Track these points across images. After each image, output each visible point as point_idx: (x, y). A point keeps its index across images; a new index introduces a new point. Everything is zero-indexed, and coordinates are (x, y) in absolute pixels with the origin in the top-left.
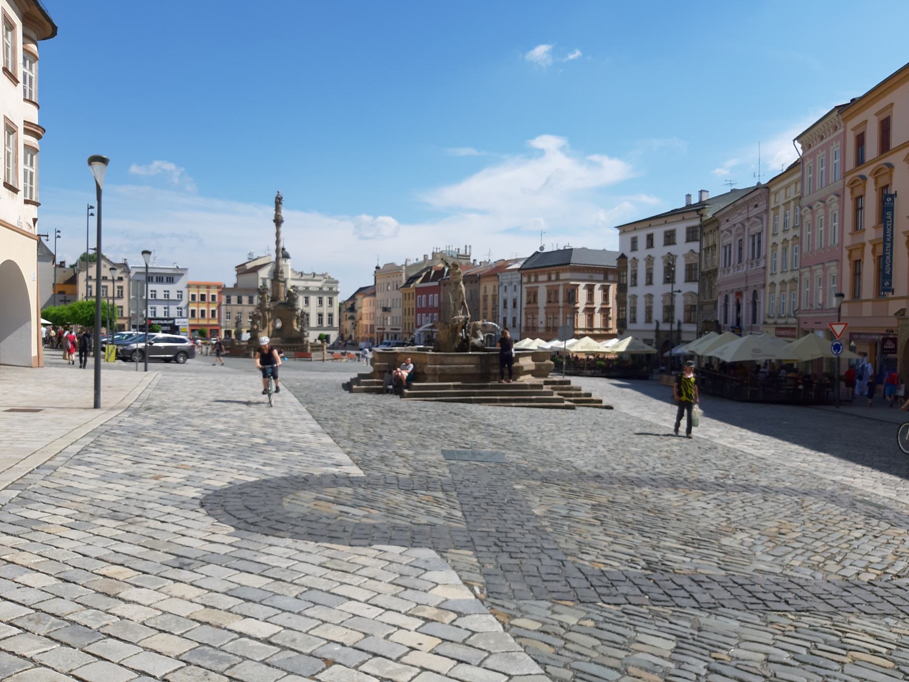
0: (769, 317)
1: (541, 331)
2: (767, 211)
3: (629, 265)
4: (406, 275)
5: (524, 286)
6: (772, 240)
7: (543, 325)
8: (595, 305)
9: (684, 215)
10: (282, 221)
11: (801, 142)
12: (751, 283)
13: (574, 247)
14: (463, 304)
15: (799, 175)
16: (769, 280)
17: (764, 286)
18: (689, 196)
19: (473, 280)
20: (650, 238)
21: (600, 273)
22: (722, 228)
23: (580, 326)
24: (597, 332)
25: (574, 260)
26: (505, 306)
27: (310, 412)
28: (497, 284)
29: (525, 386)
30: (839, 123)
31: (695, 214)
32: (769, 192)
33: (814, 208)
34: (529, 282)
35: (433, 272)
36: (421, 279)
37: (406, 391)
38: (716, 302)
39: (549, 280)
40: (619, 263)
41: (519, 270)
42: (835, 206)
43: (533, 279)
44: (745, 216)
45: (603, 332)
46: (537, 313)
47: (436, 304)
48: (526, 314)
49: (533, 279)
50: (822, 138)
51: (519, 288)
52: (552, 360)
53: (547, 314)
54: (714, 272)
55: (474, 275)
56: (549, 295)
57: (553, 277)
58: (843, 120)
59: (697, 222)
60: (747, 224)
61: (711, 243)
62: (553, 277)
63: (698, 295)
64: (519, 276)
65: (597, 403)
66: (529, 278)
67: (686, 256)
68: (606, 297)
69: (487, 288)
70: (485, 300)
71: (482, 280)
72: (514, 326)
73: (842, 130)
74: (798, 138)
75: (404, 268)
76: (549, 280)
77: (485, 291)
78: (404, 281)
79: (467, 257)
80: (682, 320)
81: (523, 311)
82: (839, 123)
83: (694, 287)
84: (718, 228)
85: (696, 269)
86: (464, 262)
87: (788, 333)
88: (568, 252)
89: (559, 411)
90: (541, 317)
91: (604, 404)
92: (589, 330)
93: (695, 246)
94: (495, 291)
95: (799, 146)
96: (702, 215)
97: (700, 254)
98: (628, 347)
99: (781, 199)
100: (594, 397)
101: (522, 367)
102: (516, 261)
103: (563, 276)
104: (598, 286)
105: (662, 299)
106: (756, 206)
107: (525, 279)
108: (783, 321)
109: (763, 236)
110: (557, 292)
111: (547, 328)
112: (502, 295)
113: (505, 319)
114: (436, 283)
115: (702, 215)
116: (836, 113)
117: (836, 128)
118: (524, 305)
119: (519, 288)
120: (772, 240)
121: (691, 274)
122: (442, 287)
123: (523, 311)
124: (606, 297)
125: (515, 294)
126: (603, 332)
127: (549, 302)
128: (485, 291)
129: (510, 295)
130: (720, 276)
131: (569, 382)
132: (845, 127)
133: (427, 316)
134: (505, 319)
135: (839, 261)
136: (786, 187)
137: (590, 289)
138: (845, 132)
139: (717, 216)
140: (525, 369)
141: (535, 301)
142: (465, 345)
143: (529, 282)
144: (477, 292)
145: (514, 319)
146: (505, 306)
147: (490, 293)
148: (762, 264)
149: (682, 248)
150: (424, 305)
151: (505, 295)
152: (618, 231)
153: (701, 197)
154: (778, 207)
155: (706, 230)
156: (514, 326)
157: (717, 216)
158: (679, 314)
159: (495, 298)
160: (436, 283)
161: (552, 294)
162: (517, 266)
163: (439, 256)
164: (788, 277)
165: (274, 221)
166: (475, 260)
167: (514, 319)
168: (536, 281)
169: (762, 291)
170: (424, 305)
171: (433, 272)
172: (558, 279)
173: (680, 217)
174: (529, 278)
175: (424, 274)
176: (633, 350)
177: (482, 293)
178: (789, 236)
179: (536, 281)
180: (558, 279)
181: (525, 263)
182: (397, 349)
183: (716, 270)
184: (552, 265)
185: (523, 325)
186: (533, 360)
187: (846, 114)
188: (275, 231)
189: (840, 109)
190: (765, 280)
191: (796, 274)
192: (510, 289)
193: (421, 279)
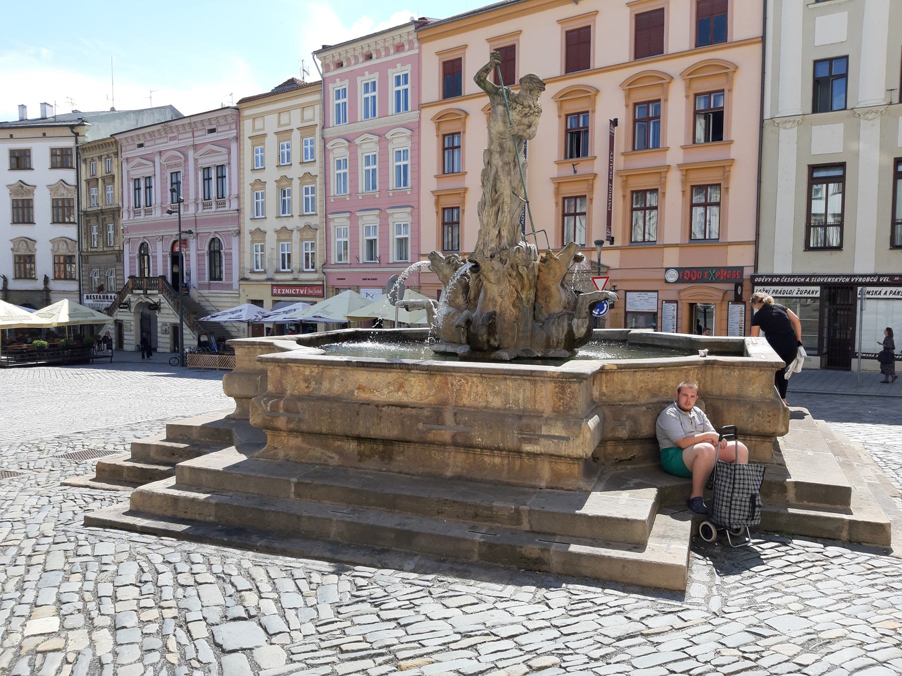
0: (252, 272)
2: (237, 138)
6: (249, 177)
9: (46, 130)
11: (323, 59)
12: (210, 231)
16: (248, 226)
17: (239, 233)
18: (22, 107)
22: (125, 155)
30: (410, 42)
31: (68, 132)
33: (357, 141)
38: (120, 253)
42: (400, 141)
44: (189, 142)
50: (369, 57)
54: (116, 213)
58: (419, 39)
59: (69, 143)
60: (191, 153)
61: (100, 171)
63: (79, 241)
67: (52, 188)
73: (416, 51)
74: (316, 53)
80: (51, 276)
82: (410, 42)
83: (71, 232)
84: (116, 154)
85: (71, 207)
87: (292, 291)
93: (69, 176)
95: (319, 62)
96: (77, 135)
97: (78, 187)
98: (69, 315)
99: (270, 125)
105: (11, 245)
108: (289, 277)
109: (232, 173)
115: (77, 135)
116: (413, 28)
117: (399, 48)
121: (61, 211)
130: (125, 218)
132: (420, 48)
135: (415, 209)
136: (303, 108)
138: (419, 55)
139: (117, 137)
148: (234, 205)
149: (43, 178)
153: (44, 111)
154: (265, 135)
155: (87, 155)
157: (117, 137)
158: (44, 265)
164: (295, 223)
169: (235, 240)
173: (39, 132)
176: (80, 320)
178: (295, 172)
183: (119, 209)
187: (424, 34)
189: (421, 24)
190: (239, 226)
191: (315, 221)
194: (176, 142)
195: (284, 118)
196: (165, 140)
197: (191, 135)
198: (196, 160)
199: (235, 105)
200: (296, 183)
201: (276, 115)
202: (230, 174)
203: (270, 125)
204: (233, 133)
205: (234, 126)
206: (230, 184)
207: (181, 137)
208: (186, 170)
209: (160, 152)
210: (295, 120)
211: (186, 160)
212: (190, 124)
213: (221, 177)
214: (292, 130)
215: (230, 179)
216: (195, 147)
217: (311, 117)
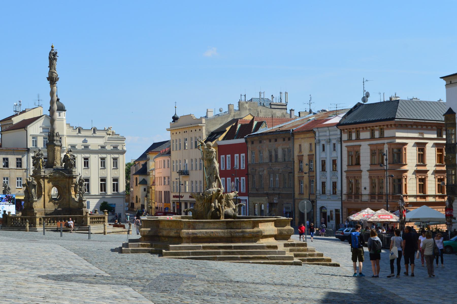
1: (365, 198)
4: (207, 130)
5: (344, 145)
7: (367, 192)
8: (427, 168)
10: (57, 79)
13: (403, 96)
14: (217, 178)
19: (288, 135)
21: (432, 129)
23: (409, 193)
24: (431, 199)
25: (400, 114)
26: (323, 169)
27: (86, 260)
28: (313, 141)
29: (262, 247)
34: (350, 139)
35: (239, 126)
36: (224, 135)
37: (164, 251)
40: (446, 119)
41: (338, 125)
43: (354, 136)
45: (419, 200)
46: (361, 177)
47: (243, 167)
48: (347, 178)
49: (354, 136)
51: (338, 146)
52: (292, 226)
53: (370, 177)
55: (287, 131)
57: (377, 134)
62: (377, 134)
64: (339, 132)
65: (328, 263)
66: (350, 136)
68: (422, 158)
69: (303, 146)
70: (301, 161)
71: (296, 137)
72: (335, 193)
75: (204, 121)
76: (373, 137)
77: (300, 151)
78: (205, 137)
79: (283, 106)
81: (344, 174)
86: (278, 113)
88: (393, 104)
89: (288, 266)
90: (365, 182)
91: (333, 262)
92: (421, 197)
94: (311, 150)
100: (324, 257)
101: (261, 232)
102: (336, 113)
103: (387, 133)
104: (430, 144)
107: (345, 137)
111: (372, 195)
112: (320, 156)
113: (324, 184)
114: (242, 141)
118: (345, 168)
119: (338, 146)
122: (249, 145)
123: (344, 174)
124: (422, 158)
125: (334, 154)
126: (419, 200)
128: (300, 151)
129: (328, 155)
131: (305, 245)
133: (233, 180)
134: (324, 184)
137: (421, 148)
140: (266, 233)
141: (358, 164)
142: (215, 215)
143: (350, 139)
144: (290, 151)
145: (334, 184)
146: (323, 169)
147: (306, 152)
150: (228, 168)
151: (323, 155)
152: (444, 82)
156: (335, 193)
159: (311, 158)
160: (242, 141)
161: (376, 153)
162: (336, 120)
163: (247, 105)
165: (48, 79)
166: (291, 110)
167: (334, 184)
168: (358, 139)
170: (228, 168)
171: (239, 126)
172: (382, 136)
174: (350, 136)
175: (228, 129)
177: (296, 153)
179: (358, 139)
180: (382, 136)
181: (344, 117)
182: (161, 218)
184: (374, 117)
185: (345, 191)
186: (276, 226)
188: (50, 90)
192: (328, 148)
193: (224, 135)
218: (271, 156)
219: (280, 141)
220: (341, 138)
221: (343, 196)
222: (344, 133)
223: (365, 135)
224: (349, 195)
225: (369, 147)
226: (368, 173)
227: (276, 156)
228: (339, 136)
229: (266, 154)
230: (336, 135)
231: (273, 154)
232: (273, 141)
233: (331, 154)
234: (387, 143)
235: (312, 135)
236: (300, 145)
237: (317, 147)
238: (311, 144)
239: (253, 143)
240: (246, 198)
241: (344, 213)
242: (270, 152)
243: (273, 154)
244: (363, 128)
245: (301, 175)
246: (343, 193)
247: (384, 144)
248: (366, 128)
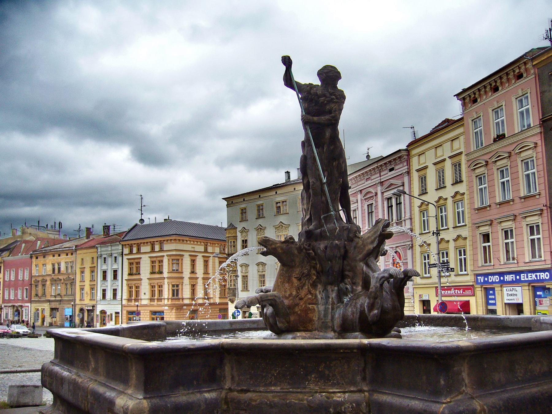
2: (408, 173)
3: (239, 234)
7: (148, 296)
8: (198, 276)
15: (461, 130)
20: (260, 208)
32: (408, 155)
34: (131, 252)
39: (153, 250)
43: (135, 250)
44: (377, 180)
47: (27, 278)
51: (120, 258)
56: (138, 269)
64: (120, 247)
76: (153, 250)
81: (125, 282)
106: (391, 170)
107: (126, 251)
110: (161, 262)
118: (126, 277)
120: (462, 188)
123: (125, 282)
125: (115, 267)
127: (153, 273)
151: (104, 267)
152: (226, 203)
154: (426, 168)
168: (139, 251)
180: (161, 250)
185: (125, 296)
192: (109, 260)
194: (369, 182)
195: (439, 151)
196: (363, 182)
197: (378, 175)
198: (383, 193)
199: (405, 148)
200: (450, 202)
201: (434, 150)
202: (404, 200)
203: (429, 159)
204: (405, 169)
205: (405, 164)
206: (405, 208)
207: (373, 177)
208: (376, 202)
209: (361, 191)
210: (446, 152)
211: (376, 194)
212: (377, 167)
213: (399, 204)
214: (444, 160)
215: (404, 204)
216: (382, 183)
217: (458, 147)
218: (54, 270)
219: (63, 256)
220: (122, 252)
221: (123, 300)
222: (126, 248)
223: (148, 248)
224: (129, 300)
225: (149, 259)
226: (148, 281)
227: (59, 269)
228: (121, 251)
229: (49, 267)
230: (118, 250)
231: (56, 267)
232: (56, 256)
233: (112, 266)
234: (167, 255)
235: (95, 250)
236: (82, 259)
237: (99, 260)
238: (93, 258)
239: (37, 258)
240: (29, 304)
241: (123, 315)
242: (53, 265)
243: (56, 267)
244: (144, 243)
245: (82, 284)
246: (123, 298)
247: (163, 256)
248: (147, 242)
